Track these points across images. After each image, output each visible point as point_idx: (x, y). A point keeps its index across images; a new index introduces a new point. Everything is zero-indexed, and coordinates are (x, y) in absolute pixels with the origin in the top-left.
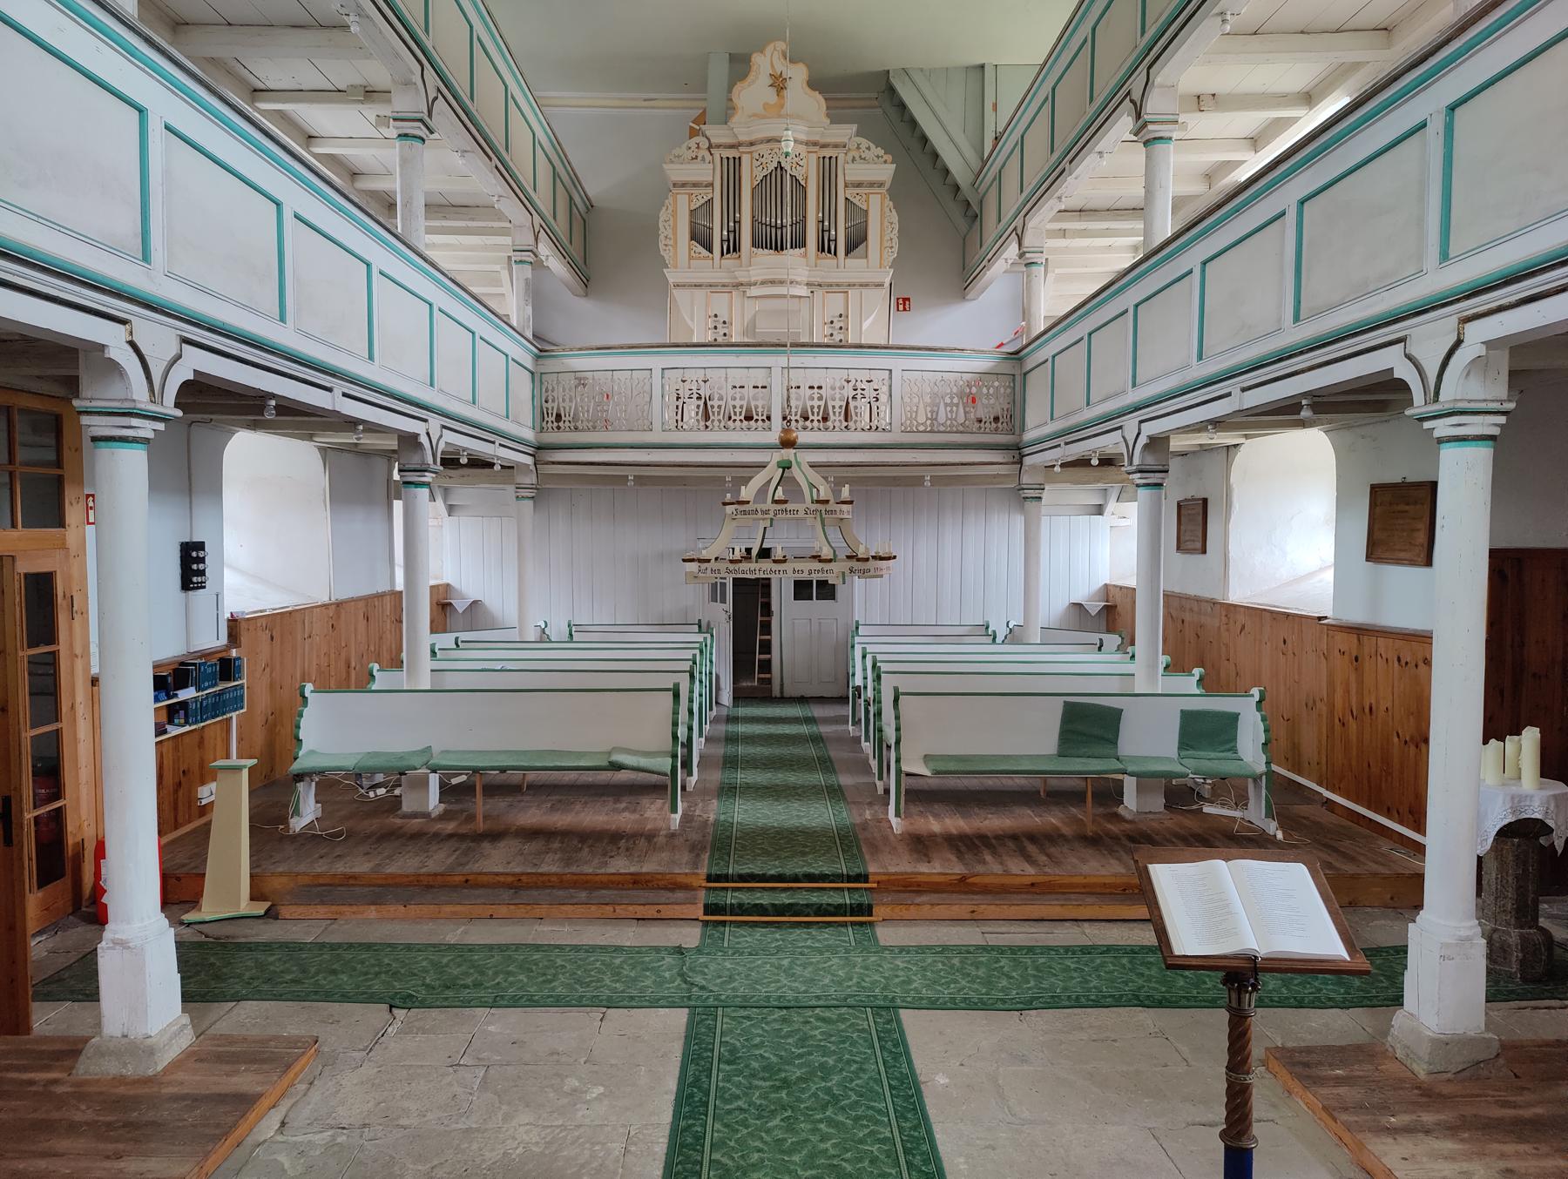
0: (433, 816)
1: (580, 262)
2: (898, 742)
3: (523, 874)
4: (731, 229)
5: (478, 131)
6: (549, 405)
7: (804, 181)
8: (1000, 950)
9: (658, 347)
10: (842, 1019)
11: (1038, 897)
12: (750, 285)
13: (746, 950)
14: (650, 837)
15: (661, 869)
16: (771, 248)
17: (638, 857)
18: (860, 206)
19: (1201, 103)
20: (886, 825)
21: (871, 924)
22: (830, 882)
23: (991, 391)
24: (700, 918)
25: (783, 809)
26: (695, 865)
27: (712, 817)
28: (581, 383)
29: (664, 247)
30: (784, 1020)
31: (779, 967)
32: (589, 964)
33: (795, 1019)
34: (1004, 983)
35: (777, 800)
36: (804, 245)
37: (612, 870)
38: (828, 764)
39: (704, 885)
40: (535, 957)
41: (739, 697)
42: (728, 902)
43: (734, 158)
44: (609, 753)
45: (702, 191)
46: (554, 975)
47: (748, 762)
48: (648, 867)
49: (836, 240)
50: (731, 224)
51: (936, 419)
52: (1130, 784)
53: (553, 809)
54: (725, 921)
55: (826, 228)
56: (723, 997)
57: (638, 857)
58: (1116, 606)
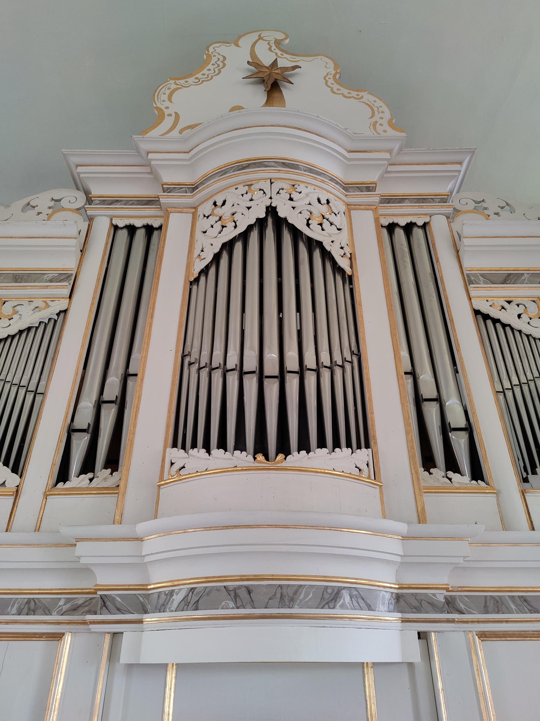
16: (240, 445)
18: (527, 329)
43: (149, 230)
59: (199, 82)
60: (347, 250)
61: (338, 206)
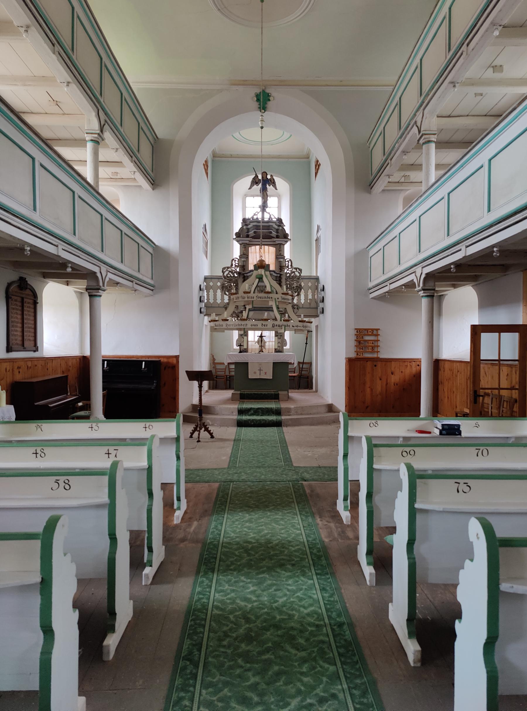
25: (263, 530)
35: (269, 542)
47: (322, 653)
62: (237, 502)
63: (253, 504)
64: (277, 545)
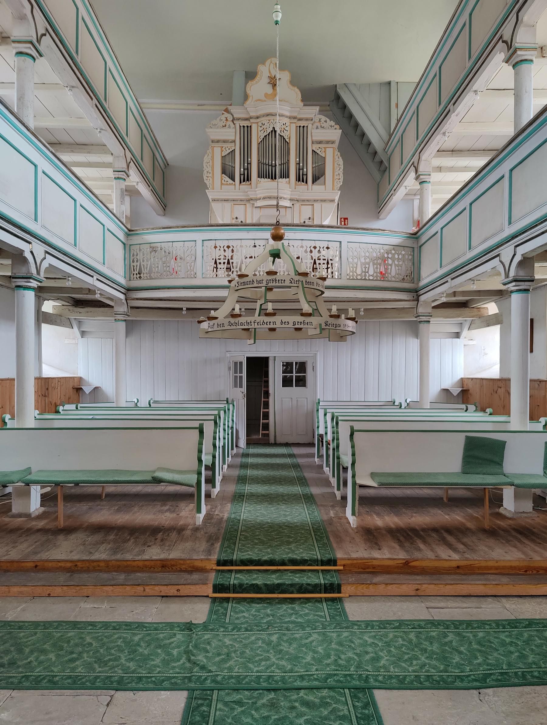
0: (33, 516)
1: (160, 193)
2: (353, 464)
3: (79, 561)
4: (246, 167)
5: (81, 75)
6: (135, 264)
7: (288, 139)
8: (446, 624)
9: (200, 226)
10: (324, 704)
11: (464, 577)
12: (257, 200)
13: (243, 626)
14: (180, 530)
15: (183, 556)
16: (269, 178)
17: (169, 546)
18: (321, 154)
19: (544, 52)
20: (345, 521)
21: (340, 600)
22: (309, 565)
23: (400, 257)
24: (210, 596)
25: (274, 510)
26: (209, 552)
27: (226, 516)
28: (154, 250)
29: (207, 178)
30: (273, 705)
31: (269, 643)
32: (112, 642)
33: (282, 704)
34: (457, 659)
35: (270, 504)
36: (288, 177)
37: (147, 557)
38: (304, 481)
39: (214, 568)
40: (69, 635)
41: (249, 443)
42: (232, 583)
43: (248, 126)
44: (154, 472)
45: (229, 145)
46: (80, 653)
47: (253, 479)
48: (174, 555)
49: (307, 175)
50: (246, 165)
51: (368, 272)
52: (508, 494)
53: (119, 511)
54: (229, 598)
55: (301, 168)
56: (219, 678)
57: (169, 546)
58: (469, 390)
59: (257, 83)
60: (289, 136)
61: (288, 124)
62: (303, 532)
63: (286, 529)
64: (266, 502)
